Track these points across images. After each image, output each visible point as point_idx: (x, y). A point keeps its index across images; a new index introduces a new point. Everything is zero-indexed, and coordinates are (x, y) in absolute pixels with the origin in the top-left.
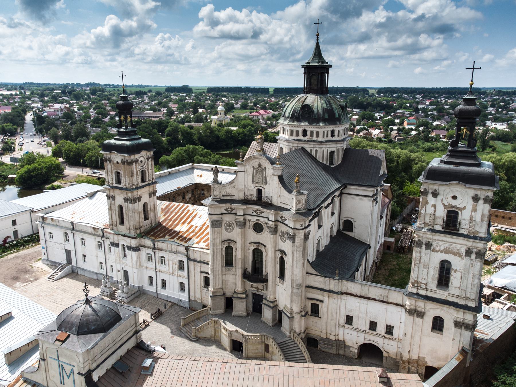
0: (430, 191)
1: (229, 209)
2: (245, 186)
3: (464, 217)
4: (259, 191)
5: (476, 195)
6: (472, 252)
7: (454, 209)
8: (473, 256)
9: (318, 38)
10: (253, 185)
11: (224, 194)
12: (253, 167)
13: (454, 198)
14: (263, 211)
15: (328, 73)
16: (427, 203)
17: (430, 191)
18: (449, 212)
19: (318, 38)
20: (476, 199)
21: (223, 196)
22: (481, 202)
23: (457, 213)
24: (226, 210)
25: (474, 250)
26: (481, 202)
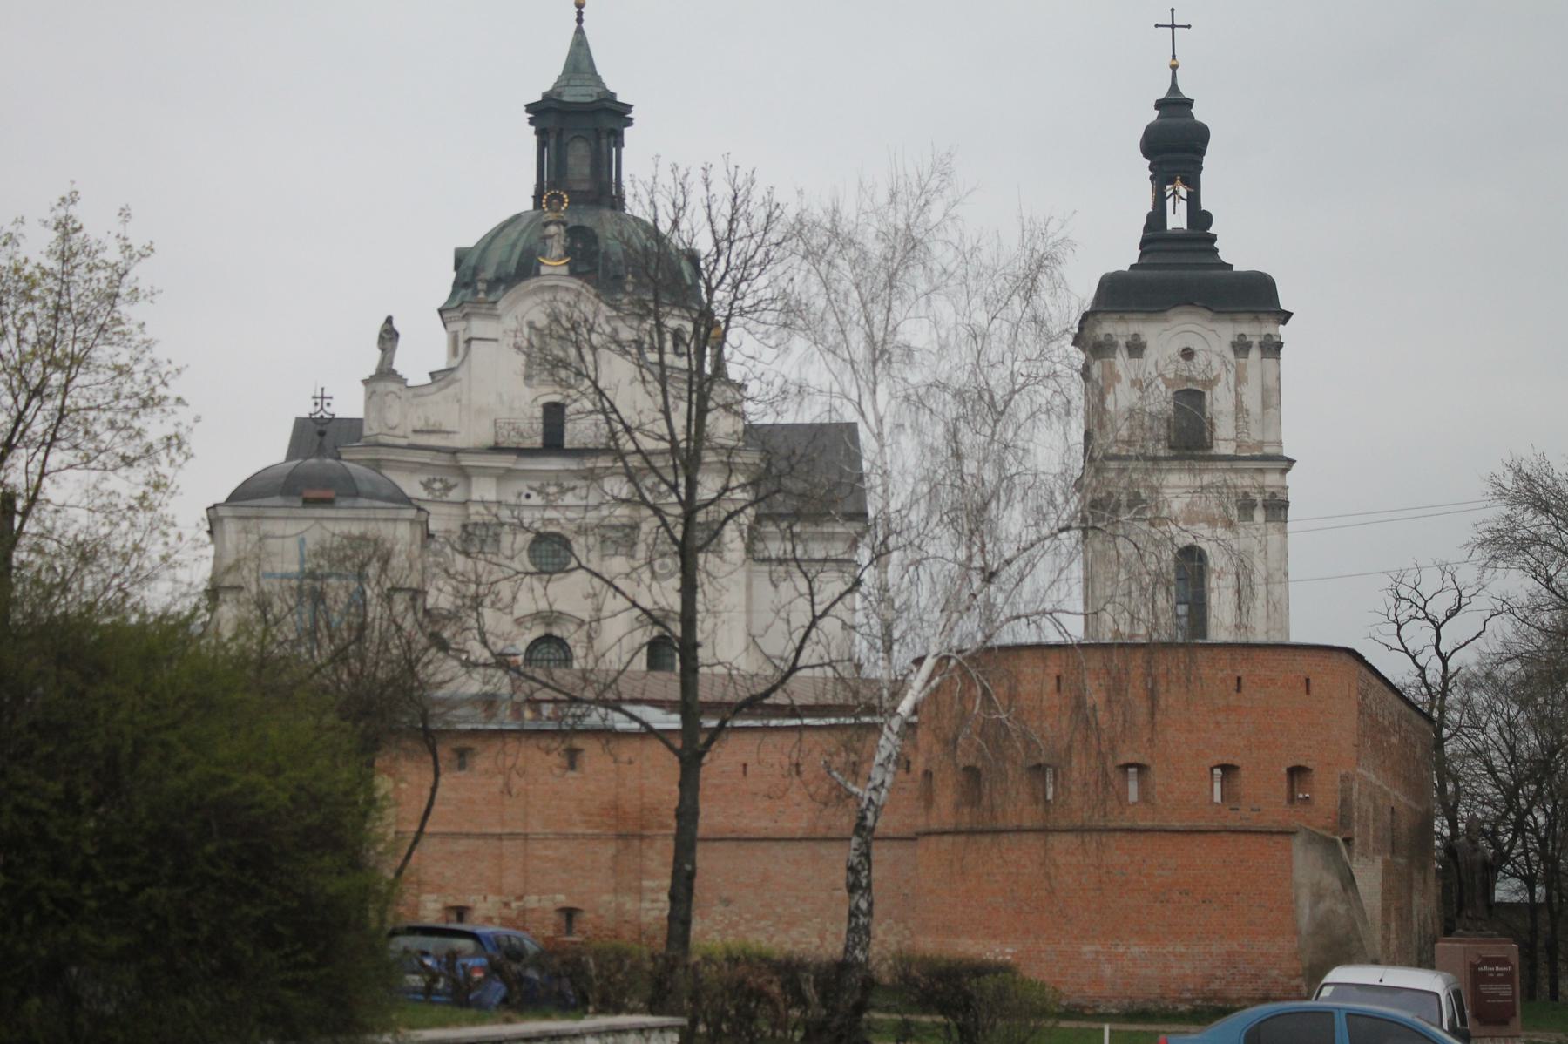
0: (1122, 342)
1: (437, 485)
2: (500, 395)
3: (1220, 402)
4: (554, 415)
5: (1243, 335)
6: (1253, 505)
7: (1190, 386)
8: (1259, 515)
9: (580, 14)
10: (527, 394)
11: (420, 425)
12: (531, 325)
13: (1188, 354)
14: (572, 484)
15: (619, 144)
16: (1117, 378)
17: (1122, 342)
18: (1179, 395)
19: (580, 14)
20: (1241, 347)
21: (415, 432)
22: (1255, 354)
23: (1202, 394)
24: (427, 486)
25: (1259, 499)
26: (1255, 354)
